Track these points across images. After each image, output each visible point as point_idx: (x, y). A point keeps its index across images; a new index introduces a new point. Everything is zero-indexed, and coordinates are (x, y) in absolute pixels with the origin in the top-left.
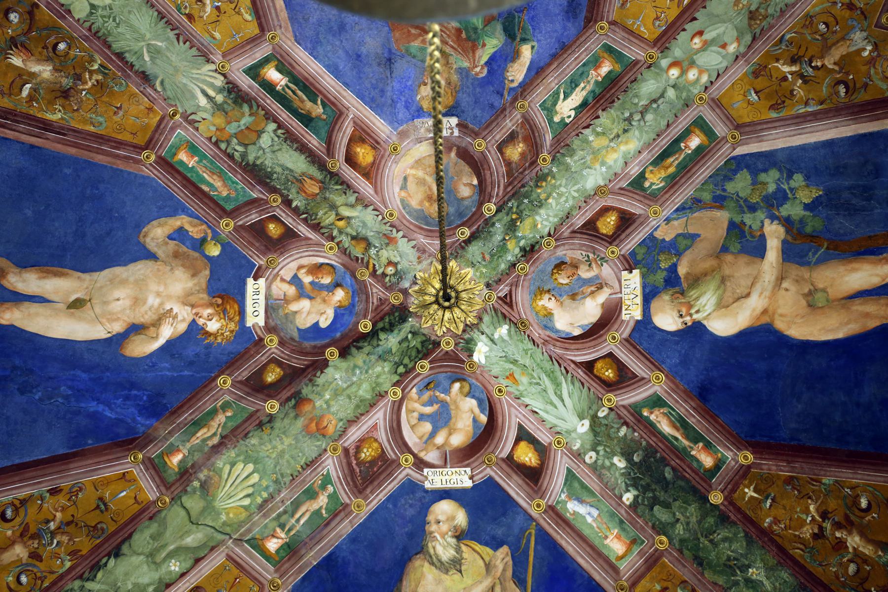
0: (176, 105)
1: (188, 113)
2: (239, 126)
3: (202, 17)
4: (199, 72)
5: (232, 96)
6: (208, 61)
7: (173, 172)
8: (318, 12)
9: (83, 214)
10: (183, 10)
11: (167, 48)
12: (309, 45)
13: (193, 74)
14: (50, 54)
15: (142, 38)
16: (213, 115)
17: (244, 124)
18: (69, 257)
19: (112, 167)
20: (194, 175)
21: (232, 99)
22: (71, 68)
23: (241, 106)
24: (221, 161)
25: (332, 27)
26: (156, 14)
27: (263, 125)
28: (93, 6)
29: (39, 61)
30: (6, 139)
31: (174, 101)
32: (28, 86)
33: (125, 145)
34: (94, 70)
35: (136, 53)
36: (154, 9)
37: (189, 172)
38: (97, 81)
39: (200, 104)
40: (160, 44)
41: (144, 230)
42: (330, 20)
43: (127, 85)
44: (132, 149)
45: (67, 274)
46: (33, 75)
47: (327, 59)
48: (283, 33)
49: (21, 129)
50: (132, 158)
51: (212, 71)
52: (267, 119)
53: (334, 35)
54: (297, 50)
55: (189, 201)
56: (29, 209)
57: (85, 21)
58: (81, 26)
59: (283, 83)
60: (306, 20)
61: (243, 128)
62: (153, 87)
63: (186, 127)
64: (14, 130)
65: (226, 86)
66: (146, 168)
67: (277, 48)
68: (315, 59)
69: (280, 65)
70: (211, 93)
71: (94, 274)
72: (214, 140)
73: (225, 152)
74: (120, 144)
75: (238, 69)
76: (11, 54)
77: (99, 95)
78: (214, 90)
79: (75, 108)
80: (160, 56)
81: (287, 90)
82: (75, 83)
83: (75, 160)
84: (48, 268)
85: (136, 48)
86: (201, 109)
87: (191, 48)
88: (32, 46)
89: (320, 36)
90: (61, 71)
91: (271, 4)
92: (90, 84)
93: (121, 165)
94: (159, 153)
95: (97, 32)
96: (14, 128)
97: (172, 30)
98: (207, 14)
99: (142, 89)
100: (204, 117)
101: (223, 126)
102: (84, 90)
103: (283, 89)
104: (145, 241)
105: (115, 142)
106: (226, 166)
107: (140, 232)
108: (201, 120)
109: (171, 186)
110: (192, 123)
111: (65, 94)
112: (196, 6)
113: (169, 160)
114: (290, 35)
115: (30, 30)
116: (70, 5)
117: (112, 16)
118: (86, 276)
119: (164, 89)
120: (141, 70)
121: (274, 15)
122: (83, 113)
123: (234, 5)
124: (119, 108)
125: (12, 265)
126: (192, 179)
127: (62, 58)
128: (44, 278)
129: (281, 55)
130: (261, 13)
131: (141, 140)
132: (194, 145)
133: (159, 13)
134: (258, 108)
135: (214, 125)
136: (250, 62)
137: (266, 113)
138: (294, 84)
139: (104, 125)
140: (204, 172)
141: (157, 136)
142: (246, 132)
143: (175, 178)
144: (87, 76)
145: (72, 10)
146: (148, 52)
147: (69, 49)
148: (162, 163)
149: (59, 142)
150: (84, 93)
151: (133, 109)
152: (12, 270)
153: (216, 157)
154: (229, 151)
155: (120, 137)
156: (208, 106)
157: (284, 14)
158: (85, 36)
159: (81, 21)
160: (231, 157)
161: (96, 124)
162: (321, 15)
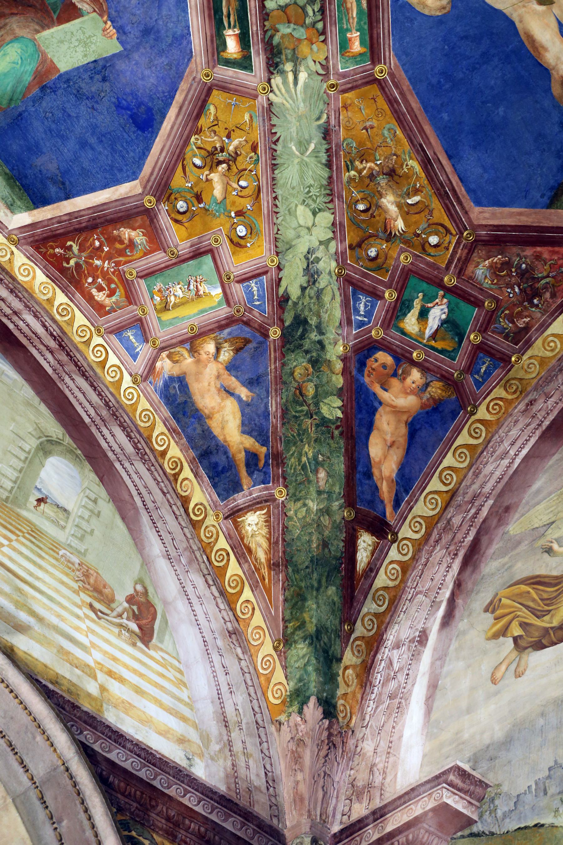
0: (325, 92)
1: (321, 78)
2: (294, 29)
3: (246, 141)
4: (285, 102)
5: (278, 60)
6: (271, 104)
7: (375, 41)
8: (156, 62)
9: (467, 72)
10: (255, 157)
11: (291, 140)
12: (185, 42)
13: (291, 105)
14: (374, 209)
15: (302, 163)
16: (305, 58)
17: (289, 27)
18: (510, 47)
19: (414, 89)
20: (362, 23)
21: (280, 58)
22: (370, 187)
23: (279, 44)
24: (333, 14)
25: (155, 40)
26: (276, 172)
27: (275, 13)
28: (314, 214)
29: (386, 211)
30: (461, 179)
31: (322, 96)
32: (409, 201)
33: (388, 97)
34: (356, 171)
35: (316, 157)
36: (274, 176)
37: (364, 29)
38: (361, 162)
39: (307, 76)
40: (294, 148)
41: (440, 14)
42: (151, 48)
43: (344, 140)
44: (386, 89)
45: (525, 33)
46: (399, 206)
47: (180, 18)
48: (197, 72)
49: (445, 176)
50: (393, 82)
51: (275, 93)
52: (268, 14)
53: (158, 31)
54: (198, 48)
55: (385, 4)
56: (498, 114)
57: (330, 209)
58: (335, 208)
59: (230, 32)
60: (170, 65)
61: (292, 25)
62: (328, 122)
63: (333, 68)
64: (449, 180)
65: (275, 72)
66: (390, 64)
67: (211, 64)
68: (189, 27)
69: (220, 50)
70: (291, 76)
71: (508, 14)
72: (322, 38)
73: (323, 19)
74: (391, 101)
75: (255, 76)
76: (399, 231)
77: (370, 151)
78: (287, 77)
79: (395, 157)
80: (302, 139)
81: (232, 23)
82: (378, 175)
83: (433, 120)
84: (532, 52)
85: (313, 159)
86: (310, 72)
87: (274, 125)
88: (380, 225)
89: (170, 41)
90: (378, 192)
91: (187, 103)
92: (369, 165)
93: (406, 84)
94: (371, 66)
95: (328, 195)
96: (448, 182)
97: (276, 151)
98: (241, 139)
99: (337, 127)
100: (313, 63)
101: (305, 42)
102: (376, 164)
103: (235, 27)
104: (448, 3)
105: (393, 106)
106: (333, 6)
107: (444, 15)
108: (317, 63)
109: (386, 31)
110: (325, 67)
111: (391, 173)
112: (243, 152)
113: (368, 54)
114: (192, 65)
115: (371, 236)
116: (329, 228)
117: (307, 196)
118: (515, 18)
119: (322, 112)
120: (324, 142)
121: (191, 92)
122: (394, 149)
123: (214, 128)
124: (366, 128)
125: (552, 80)
126: (367, 21)
127: (369, 199)
128: (543, 47)
129: (213, 56)
130: (200, 103)
131: (374, 90)
132: (341, 48)
133: (273, 171)
134: (267, 30)
135: (311, 49)
136: (241, 73)
137: (265, 20)
138: (222, 23)
139: (388, 126)
140: (353, 18)
141: (360, 82)
142: (293, 20)
143: (378, 35)
144: (365, 172)
145: (330, 224)
146: (307, 149)
147: (358, 201)
148: (376, 60)
149: (429, 144)
150: (378, 162)
151: (357, 118)
152: (556, 76)
153: (333, 22)
154: (320, 17)
155: (386, 107)
156: (302, 68)
157: (183, 86)
158: (339, 200)
159: (332, 211)
160: (322, 10)
161: (393, 132)
162: (155, 58)
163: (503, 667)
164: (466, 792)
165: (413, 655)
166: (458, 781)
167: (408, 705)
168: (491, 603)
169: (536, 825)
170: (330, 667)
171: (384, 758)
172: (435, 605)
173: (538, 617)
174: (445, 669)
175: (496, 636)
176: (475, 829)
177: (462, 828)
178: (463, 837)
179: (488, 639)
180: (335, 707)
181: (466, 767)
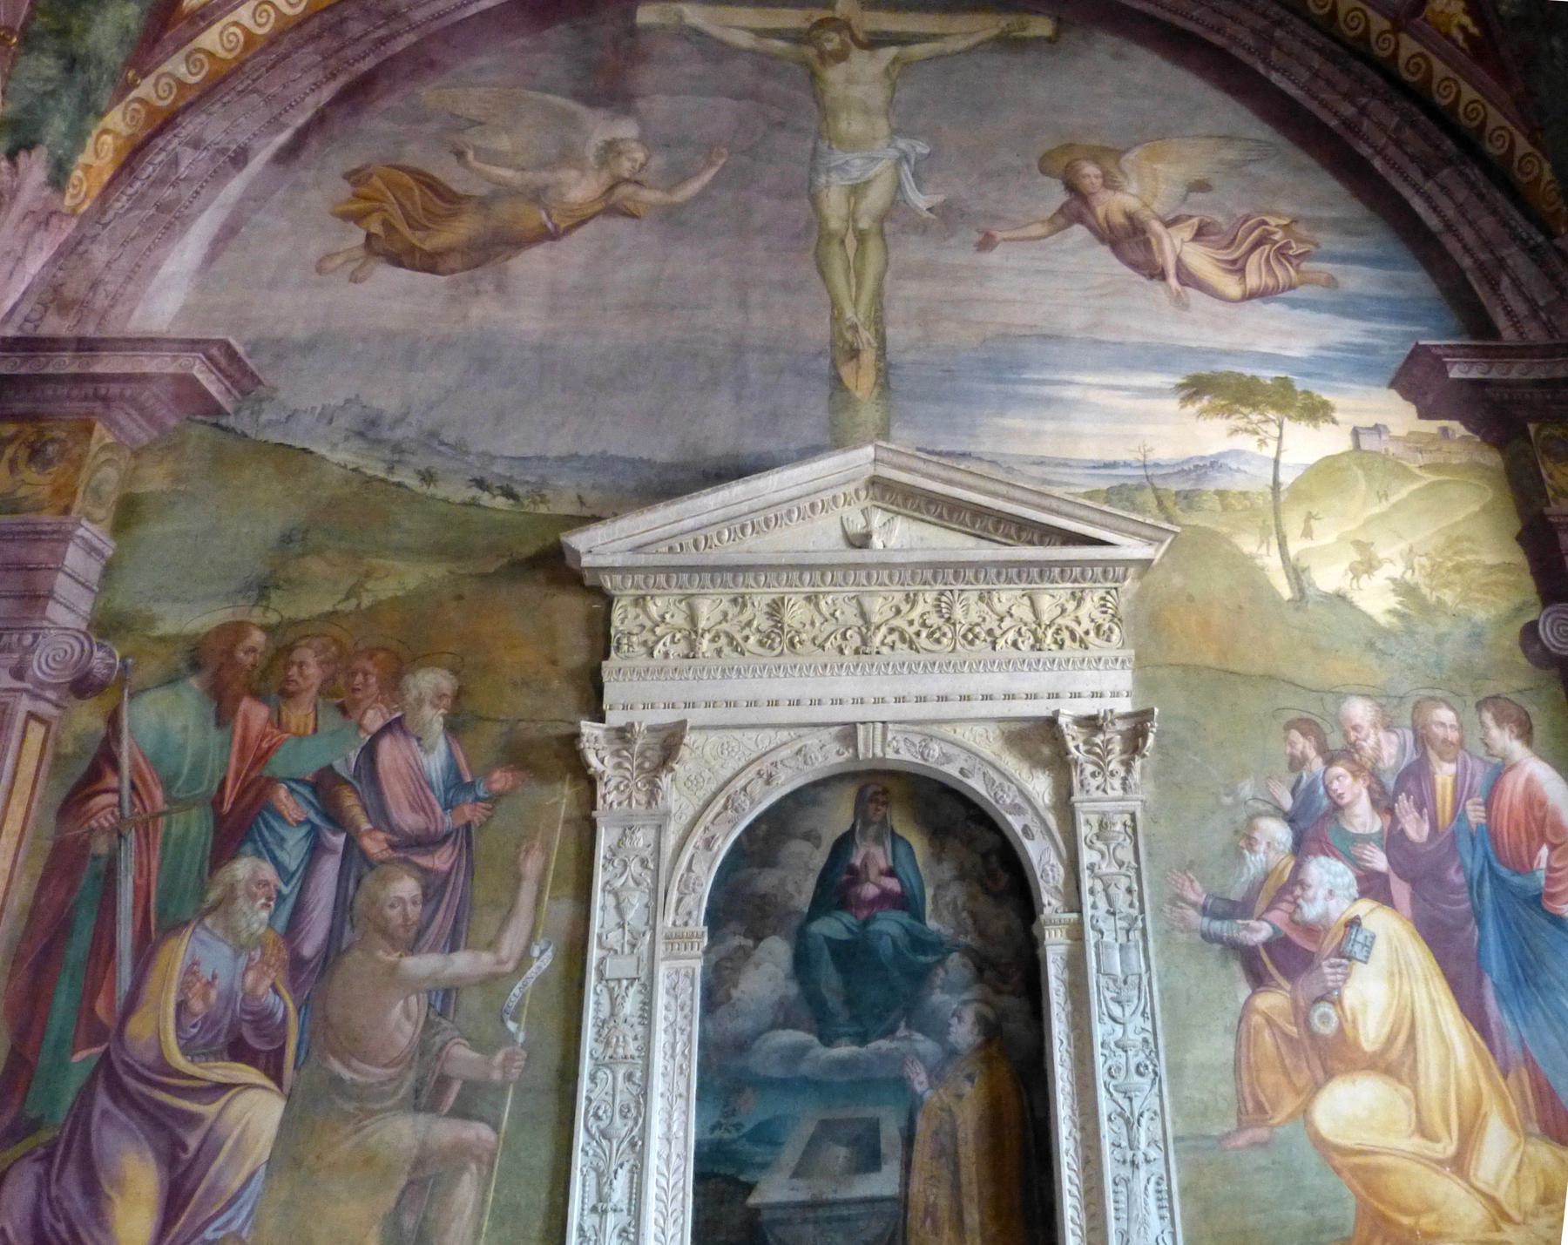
163: (338, 261)
164: (228, 377)
165: (215, 171)
166: (223, 362)
167: (184, 232)
168: (356, 172)
169: (304, 450)
170: (82, 119)
171: (121, 280)
172: (275, 124)
173: (410, 226)
174: (256, 218)
175: (346, 216)
176: (223, 421)
177: (207, 413)
178: (204, 423)
179: (334, 214)
180: (67, 175)
181: (240, 349)
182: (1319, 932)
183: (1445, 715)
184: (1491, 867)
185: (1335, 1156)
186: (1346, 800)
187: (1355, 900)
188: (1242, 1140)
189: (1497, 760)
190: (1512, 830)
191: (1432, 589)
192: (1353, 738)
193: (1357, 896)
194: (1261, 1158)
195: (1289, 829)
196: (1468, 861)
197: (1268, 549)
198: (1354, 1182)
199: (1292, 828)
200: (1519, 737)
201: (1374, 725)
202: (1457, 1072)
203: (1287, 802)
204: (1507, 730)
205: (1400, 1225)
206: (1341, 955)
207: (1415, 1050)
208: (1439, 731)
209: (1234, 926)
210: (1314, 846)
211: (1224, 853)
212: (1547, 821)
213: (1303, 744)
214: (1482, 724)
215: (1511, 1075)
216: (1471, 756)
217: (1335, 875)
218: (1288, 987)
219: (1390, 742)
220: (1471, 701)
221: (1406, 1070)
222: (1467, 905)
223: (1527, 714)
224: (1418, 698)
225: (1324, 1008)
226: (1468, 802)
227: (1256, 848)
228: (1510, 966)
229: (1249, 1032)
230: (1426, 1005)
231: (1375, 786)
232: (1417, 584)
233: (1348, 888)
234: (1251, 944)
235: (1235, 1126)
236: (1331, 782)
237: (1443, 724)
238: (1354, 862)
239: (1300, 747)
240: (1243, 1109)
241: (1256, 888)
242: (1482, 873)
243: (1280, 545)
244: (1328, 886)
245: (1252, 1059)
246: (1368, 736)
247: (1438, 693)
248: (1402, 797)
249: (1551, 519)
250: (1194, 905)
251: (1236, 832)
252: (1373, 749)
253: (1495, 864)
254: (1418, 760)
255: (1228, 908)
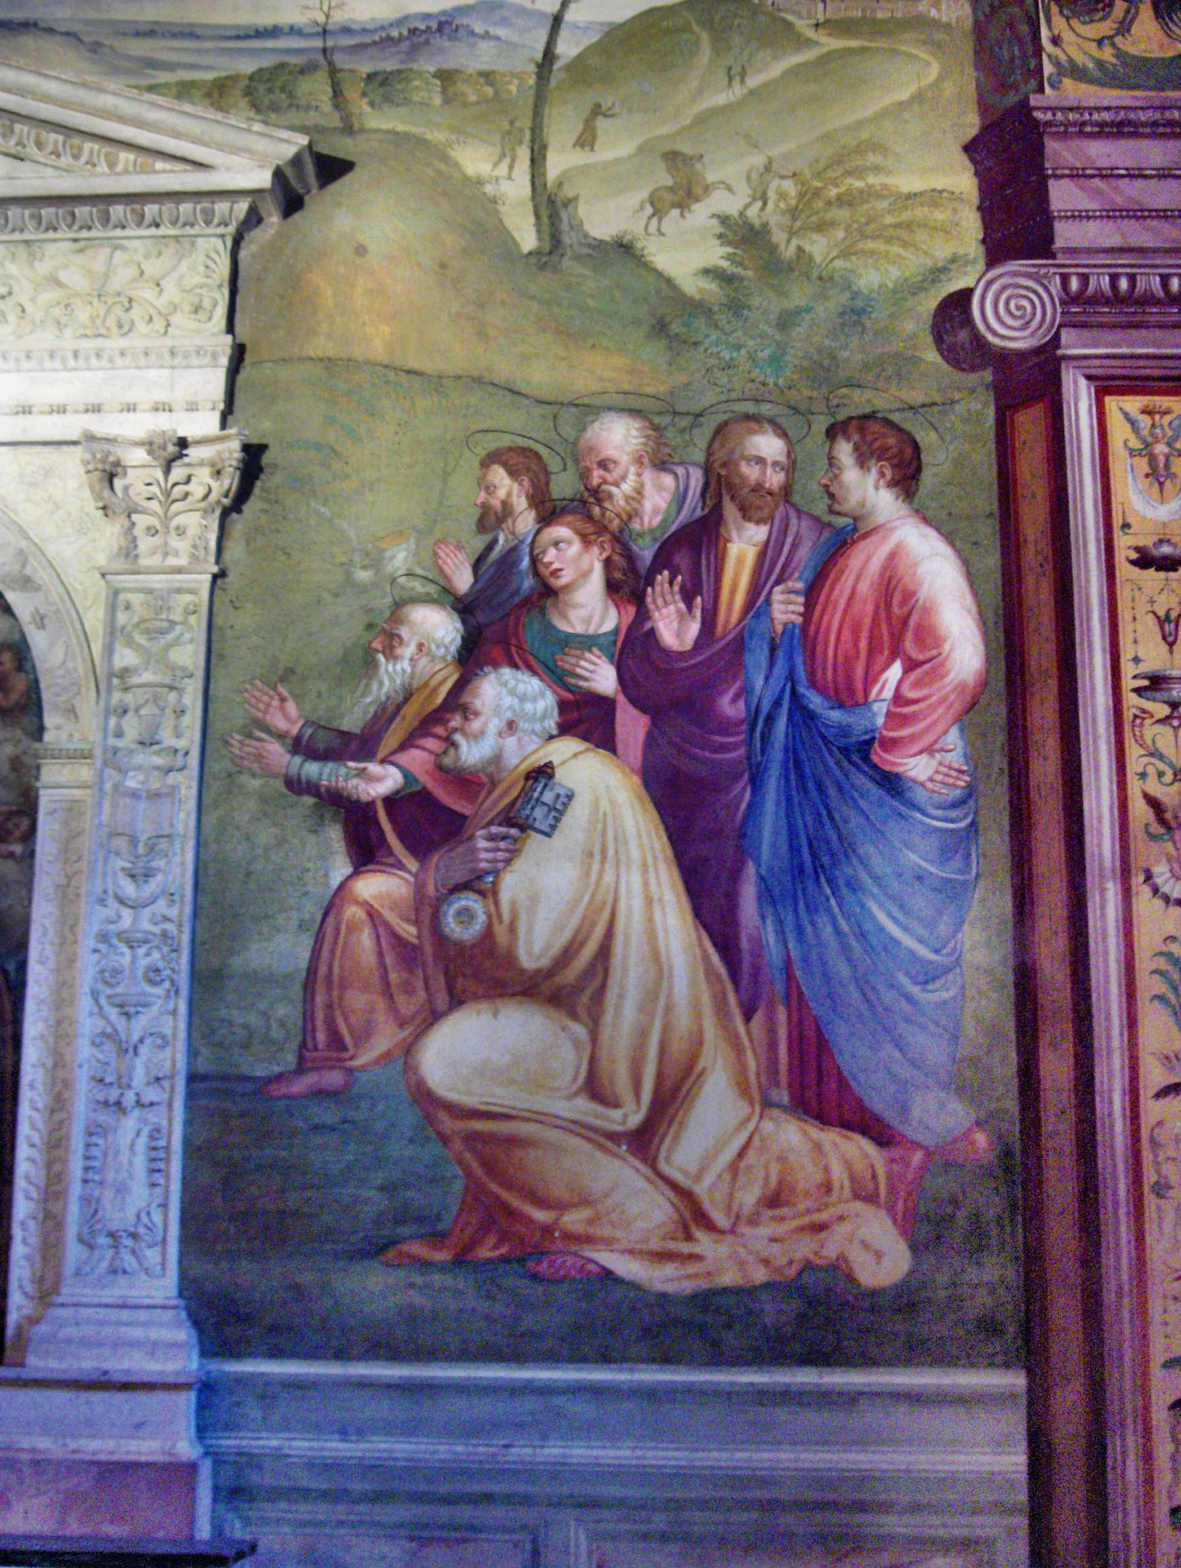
182: (481, 785)
183: (768, 445)
184: (795, 696)
185: (443, 1116)
186: (564, 580)
187: (552, 737)
188: (300, 1086)
189: (841, 521)
190: (846, 633)
191: (792, 233)
192: (595, 481)
193: (555, 732)
194: (329, 1115)
195: (459, 625)
196: (759, 682)
197: (511, 167)
198: (468, 1156)
199: (464, 622)
200: (893, 484)
201: (639, 461)
202: (668, 1009)
203: (463, 581)
204: (874, 472)
205: (530, 1221)
206: (509, 822)
207: (606, 971)
208: (751, 472)
209: (343, 771)
210: (497, 652)
211: (345, 660)
212: (912, 622)
213: (503, 483)
214: (831, 459)
215: (758, 1018)
216: (799, 512)
217: (523, 698)
218: (413, 865)
219: (659, 487)
220: (821, 423)
221: (585, 998)
222: (742, 751)
223: (916, 447)
224: (725, 417)
225: (469, 900)
226: (778, 589)
227: (399, 651)
228: (794, 848)
229: (337, 930)
230: (638, 904)
231: (617, 558)
232: (765, 225)
233: (544, 717)
234: (365, 798)
235: (293, 1067)
236: (544, 552)
237: (761, 461)
238: (556, 676)
239: (502, 493)
240: (310, 1045)
241: (386, 715)
242: (777, 703)
243: (533, 161)
244: (509, 715)
245: (336, 971)
246: (623, 478)
247: (765, 409)
248: (663, 577)
249: (1038, 115)
250: (281, 736)
251: (370, 626)
252: (628, 499)
253: (801, 689)
254: (703, 520)
255: (337, 743)
